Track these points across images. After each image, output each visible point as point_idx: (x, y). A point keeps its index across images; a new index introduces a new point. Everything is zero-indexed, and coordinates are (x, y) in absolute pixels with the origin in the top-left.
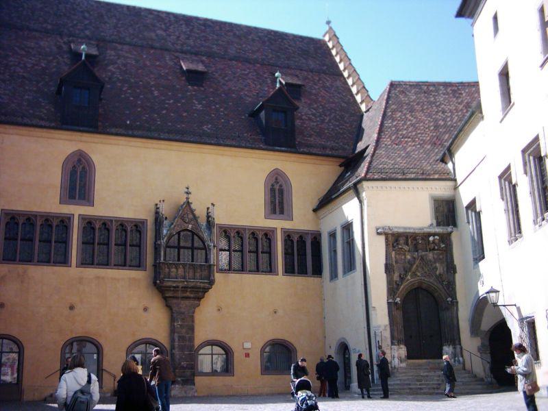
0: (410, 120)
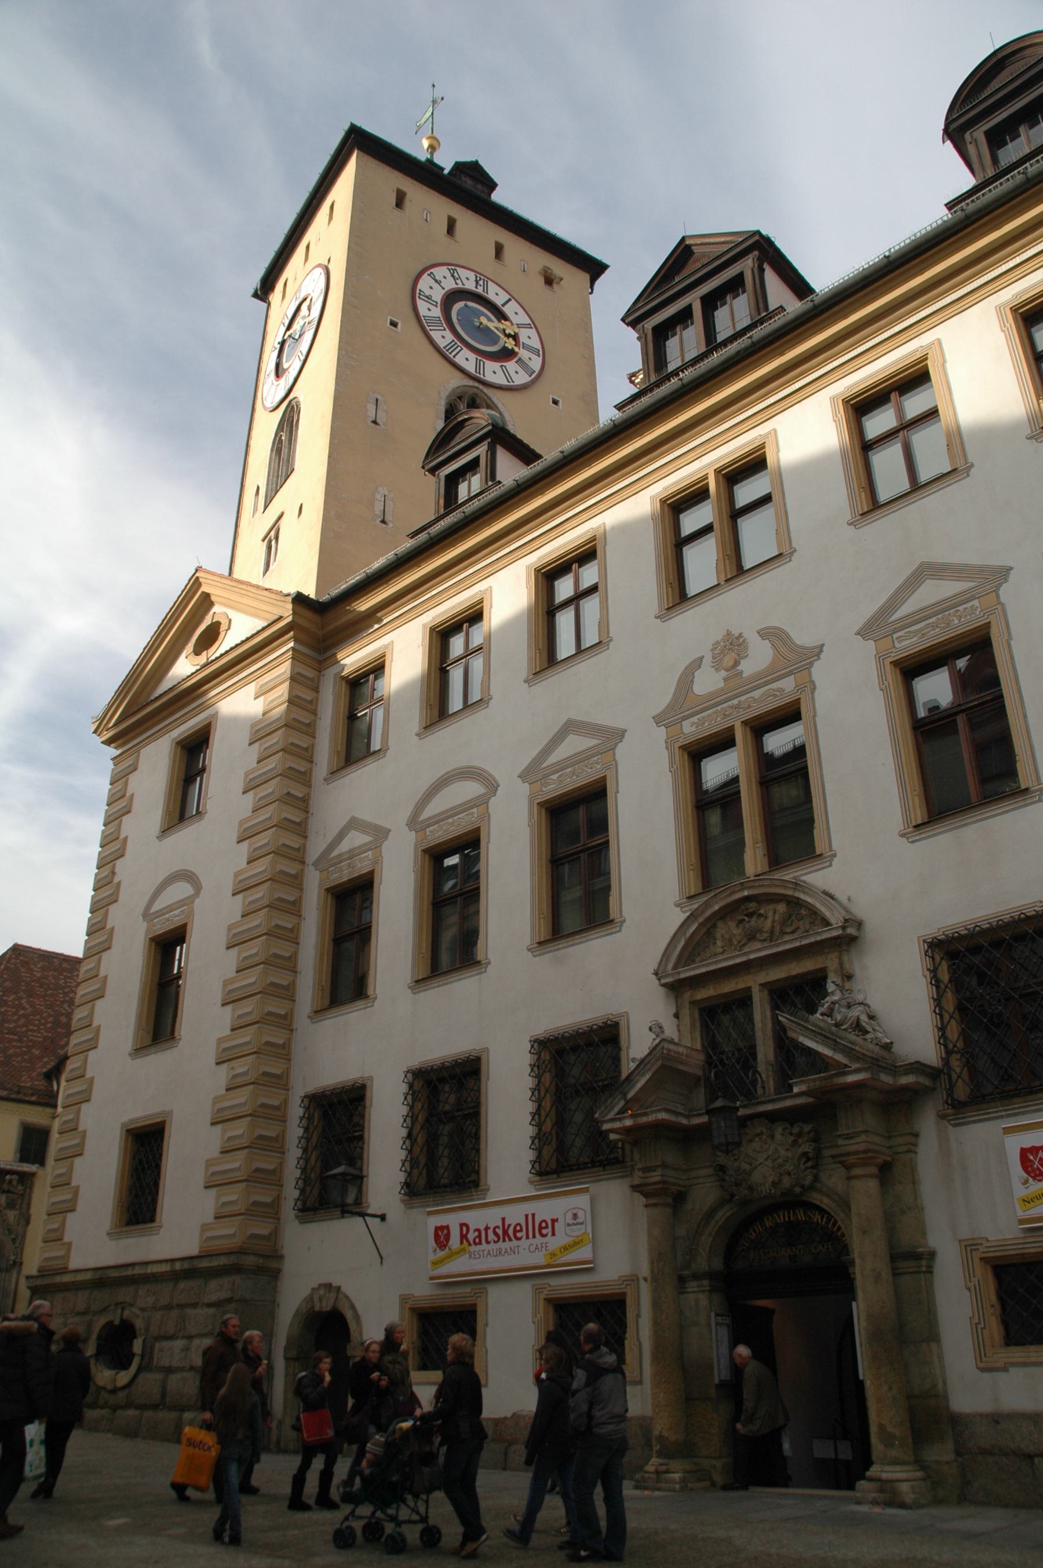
0: (24, 1009)
